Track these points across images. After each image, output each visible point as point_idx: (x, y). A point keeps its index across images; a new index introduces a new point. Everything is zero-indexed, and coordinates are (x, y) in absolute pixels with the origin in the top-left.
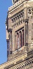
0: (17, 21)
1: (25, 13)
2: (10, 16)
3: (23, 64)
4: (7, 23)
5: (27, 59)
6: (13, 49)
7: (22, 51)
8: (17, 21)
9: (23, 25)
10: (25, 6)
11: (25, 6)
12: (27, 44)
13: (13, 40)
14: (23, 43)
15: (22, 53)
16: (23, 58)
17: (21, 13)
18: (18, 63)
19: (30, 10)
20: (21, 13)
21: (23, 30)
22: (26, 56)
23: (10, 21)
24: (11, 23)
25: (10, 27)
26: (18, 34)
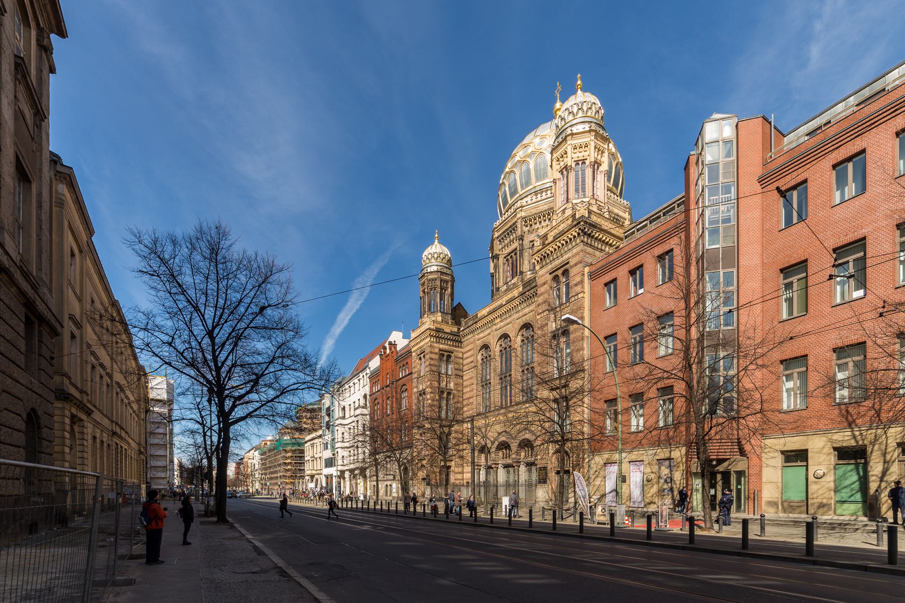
0: (506, 242)
1: (519, 226)
2: (496, 235)
3: (517, 302)
4: (492, 248)
5: (522, 294)
6: (501, 284)
7: (514, 284)
8: (506, 242)
9: (516, 245)
10: (519, 216)
11: (519, 216)
12: (521, 273)
13: (501, 271)
14: (515, 271)
15: (515, 286)
16: (515, 293)
17: (513, 228)
18: (508, 302)
19: (526, 222)
20: (513, 228)
21: (516, 254)
22: (521, 289)
23: (496, 242)
24: (497, 246)
25: (496, 252)
26: (507, 260)
